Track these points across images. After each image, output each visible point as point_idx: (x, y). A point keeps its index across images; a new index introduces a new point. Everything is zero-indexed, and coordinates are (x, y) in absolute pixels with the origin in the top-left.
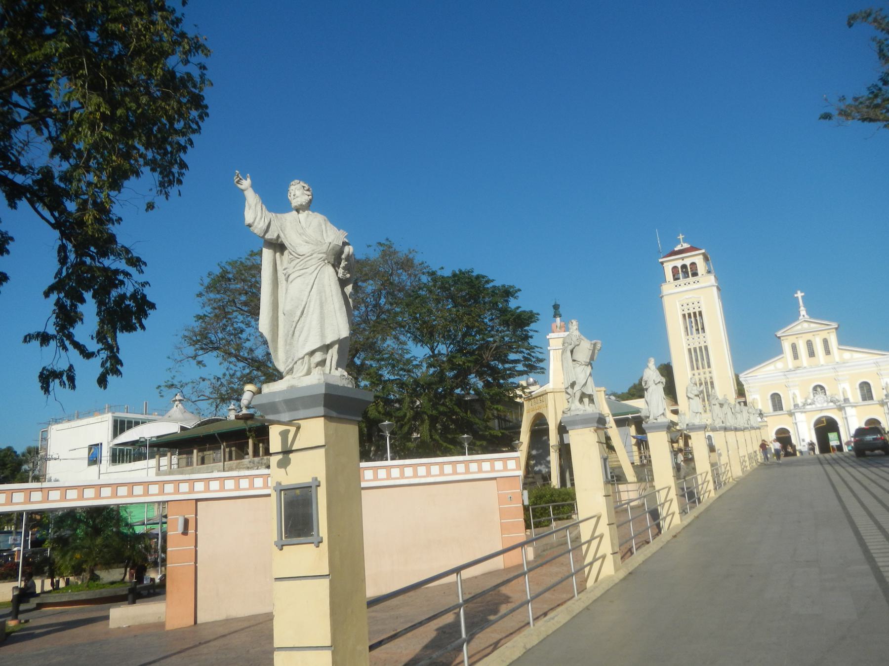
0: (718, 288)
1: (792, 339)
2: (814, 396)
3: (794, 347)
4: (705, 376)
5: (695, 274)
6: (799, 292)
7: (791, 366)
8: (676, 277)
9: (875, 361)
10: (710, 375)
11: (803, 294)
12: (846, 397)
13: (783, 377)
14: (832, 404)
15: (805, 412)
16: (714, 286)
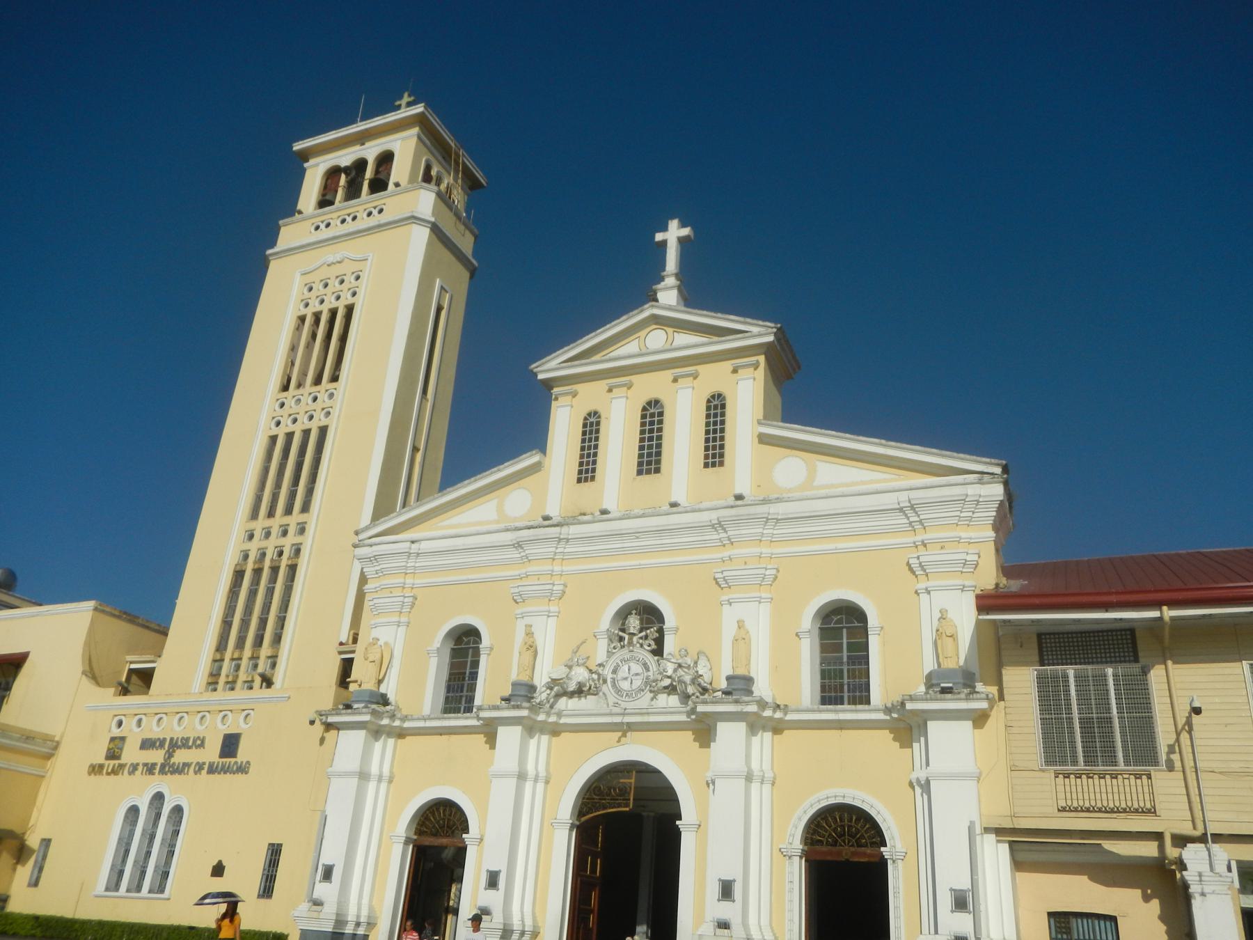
0: (435, 229)
1: (590, 396)
2: (610, 654)
3: (591, 428)
4: (282, 541)
5: (379, 185)
6: (674, 224)
7: (554, 511)
8: (328, 197)
9: (903, 497)
10: (298, 539)
11: (686, 231)
12: (741, 671)
13: (515, 554)
14: (674, 700)
15: (555, 731)
16: (414, 219)
